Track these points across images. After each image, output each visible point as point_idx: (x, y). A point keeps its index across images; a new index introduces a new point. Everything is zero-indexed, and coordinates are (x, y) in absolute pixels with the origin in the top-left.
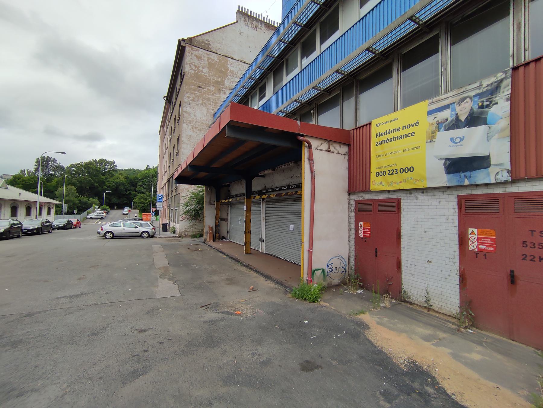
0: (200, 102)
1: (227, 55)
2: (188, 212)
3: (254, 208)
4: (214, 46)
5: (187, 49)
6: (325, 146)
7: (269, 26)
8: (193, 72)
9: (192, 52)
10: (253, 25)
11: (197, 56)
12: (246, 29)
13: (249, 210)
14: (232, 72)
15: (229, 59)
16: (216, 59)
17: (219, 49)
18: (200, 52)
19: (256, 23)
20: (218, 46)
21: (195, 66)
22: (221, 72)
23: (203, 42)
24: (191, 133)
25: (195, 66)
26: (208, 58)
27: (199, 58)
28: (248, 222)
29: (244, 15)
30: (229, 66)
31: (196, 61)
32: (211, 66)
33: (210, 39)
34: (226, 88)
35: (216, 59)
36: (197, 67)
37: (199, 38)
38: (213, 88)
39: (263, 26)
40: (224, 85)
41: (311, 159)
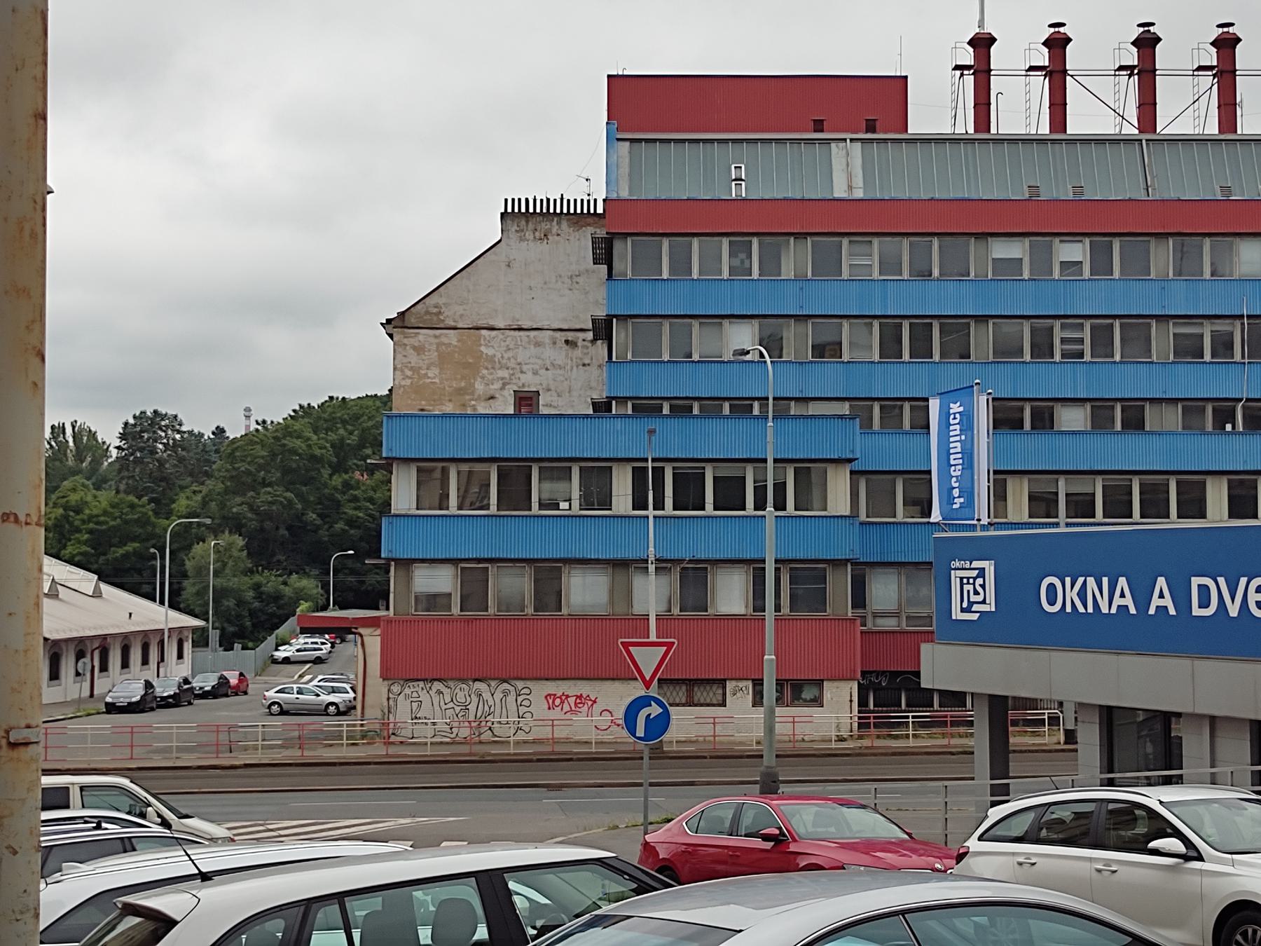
1: (481, 323)
8: (408, 382)
9: (406, 341)
10: (537, 234)
11: (414, 348)
15: (484, 332)
16: (454, 342)
17: (461, 316)
18: (421, 338)
19: (545, 226)
20: (460, 310)
21: (412, 369)
22: (467, 365)
23: (427, 313)
26: (438, 345)
29: (518, 217)
30: (483, 348)
33: (441, 301)
34: (478, 399)
35: (454, 342)
39: (564, 224)
40: (473, 393)
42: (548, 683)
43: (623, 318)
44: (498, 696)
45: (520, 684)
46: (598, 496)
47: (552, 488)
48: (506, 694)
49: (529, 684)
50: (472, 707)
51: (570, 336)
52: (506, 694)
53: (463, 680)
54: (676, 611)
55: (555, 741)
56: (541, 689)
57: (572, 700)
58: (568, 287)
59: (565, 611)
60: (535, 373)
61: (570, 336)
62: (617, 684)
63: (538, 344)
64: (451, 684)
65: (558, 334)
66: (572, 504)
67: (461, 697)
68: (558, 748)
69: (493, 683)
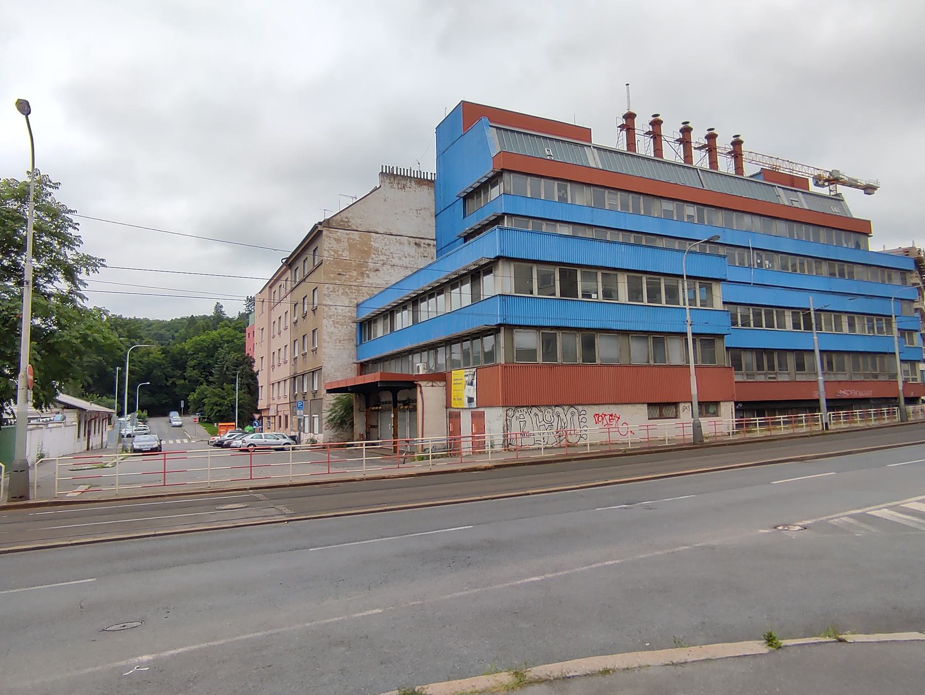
0: (341, 291)
1: (370, 229)
2: (332, 420)
3: (399, 413)
4: (354, 223)
5: (324, 233)
6: (430, 384)
7: (421, 181)
11: (335, 239)
12: (392, 192)
13: (395, 418)
14: (377, 250)
21: (334, 251)
23: (342, 221)
24: (332, 329)
25: (334, 251)
27: (338, 241)
28: (395, 427)
31: (335, 245)
32: (351, 247)
33: (349, 216)
34: (370, 270)
36: (336, 252)
37: (338, 217)
38: (355, 274)
39: (413, 183)
40: (367, 267)
41: (421, 392)
42: (595, 407)
43: (511, 215)
44: (569, 416)
45: (580, 408)
46: (609, 294)
47: (590, 285)
48: (573, 414)
49: (585, 408)
50: (555, 424)
51: (418, 240)
52: (573, 414)
53: (549, 406)
54: (652, 363)
55: (609, 443)
56: (592, 411)
57: (607, 417)
58: (415, 215)
59: (598, 362)
60: (400, 259)
61: (418, 240)
62: (629, 407)
63: (401, 243)
64: (542, 409)
65: (411, 239)
66: (598, 296)
67: (548, 418)
68: (613, 448)
69: (566, 408)
